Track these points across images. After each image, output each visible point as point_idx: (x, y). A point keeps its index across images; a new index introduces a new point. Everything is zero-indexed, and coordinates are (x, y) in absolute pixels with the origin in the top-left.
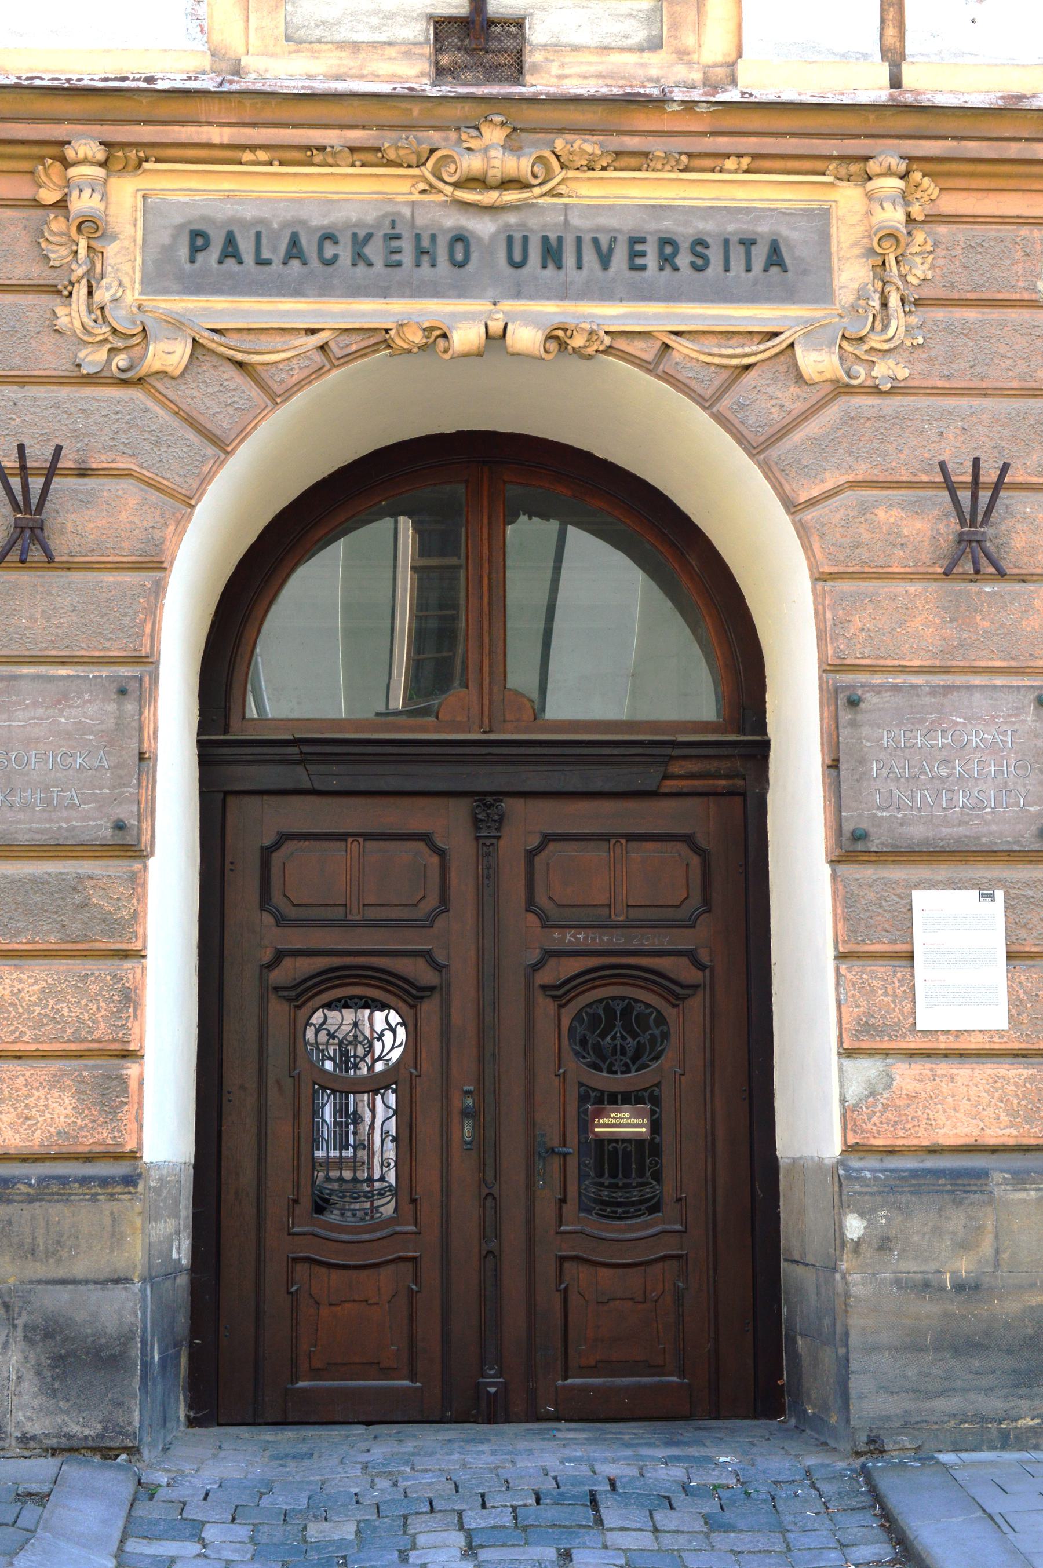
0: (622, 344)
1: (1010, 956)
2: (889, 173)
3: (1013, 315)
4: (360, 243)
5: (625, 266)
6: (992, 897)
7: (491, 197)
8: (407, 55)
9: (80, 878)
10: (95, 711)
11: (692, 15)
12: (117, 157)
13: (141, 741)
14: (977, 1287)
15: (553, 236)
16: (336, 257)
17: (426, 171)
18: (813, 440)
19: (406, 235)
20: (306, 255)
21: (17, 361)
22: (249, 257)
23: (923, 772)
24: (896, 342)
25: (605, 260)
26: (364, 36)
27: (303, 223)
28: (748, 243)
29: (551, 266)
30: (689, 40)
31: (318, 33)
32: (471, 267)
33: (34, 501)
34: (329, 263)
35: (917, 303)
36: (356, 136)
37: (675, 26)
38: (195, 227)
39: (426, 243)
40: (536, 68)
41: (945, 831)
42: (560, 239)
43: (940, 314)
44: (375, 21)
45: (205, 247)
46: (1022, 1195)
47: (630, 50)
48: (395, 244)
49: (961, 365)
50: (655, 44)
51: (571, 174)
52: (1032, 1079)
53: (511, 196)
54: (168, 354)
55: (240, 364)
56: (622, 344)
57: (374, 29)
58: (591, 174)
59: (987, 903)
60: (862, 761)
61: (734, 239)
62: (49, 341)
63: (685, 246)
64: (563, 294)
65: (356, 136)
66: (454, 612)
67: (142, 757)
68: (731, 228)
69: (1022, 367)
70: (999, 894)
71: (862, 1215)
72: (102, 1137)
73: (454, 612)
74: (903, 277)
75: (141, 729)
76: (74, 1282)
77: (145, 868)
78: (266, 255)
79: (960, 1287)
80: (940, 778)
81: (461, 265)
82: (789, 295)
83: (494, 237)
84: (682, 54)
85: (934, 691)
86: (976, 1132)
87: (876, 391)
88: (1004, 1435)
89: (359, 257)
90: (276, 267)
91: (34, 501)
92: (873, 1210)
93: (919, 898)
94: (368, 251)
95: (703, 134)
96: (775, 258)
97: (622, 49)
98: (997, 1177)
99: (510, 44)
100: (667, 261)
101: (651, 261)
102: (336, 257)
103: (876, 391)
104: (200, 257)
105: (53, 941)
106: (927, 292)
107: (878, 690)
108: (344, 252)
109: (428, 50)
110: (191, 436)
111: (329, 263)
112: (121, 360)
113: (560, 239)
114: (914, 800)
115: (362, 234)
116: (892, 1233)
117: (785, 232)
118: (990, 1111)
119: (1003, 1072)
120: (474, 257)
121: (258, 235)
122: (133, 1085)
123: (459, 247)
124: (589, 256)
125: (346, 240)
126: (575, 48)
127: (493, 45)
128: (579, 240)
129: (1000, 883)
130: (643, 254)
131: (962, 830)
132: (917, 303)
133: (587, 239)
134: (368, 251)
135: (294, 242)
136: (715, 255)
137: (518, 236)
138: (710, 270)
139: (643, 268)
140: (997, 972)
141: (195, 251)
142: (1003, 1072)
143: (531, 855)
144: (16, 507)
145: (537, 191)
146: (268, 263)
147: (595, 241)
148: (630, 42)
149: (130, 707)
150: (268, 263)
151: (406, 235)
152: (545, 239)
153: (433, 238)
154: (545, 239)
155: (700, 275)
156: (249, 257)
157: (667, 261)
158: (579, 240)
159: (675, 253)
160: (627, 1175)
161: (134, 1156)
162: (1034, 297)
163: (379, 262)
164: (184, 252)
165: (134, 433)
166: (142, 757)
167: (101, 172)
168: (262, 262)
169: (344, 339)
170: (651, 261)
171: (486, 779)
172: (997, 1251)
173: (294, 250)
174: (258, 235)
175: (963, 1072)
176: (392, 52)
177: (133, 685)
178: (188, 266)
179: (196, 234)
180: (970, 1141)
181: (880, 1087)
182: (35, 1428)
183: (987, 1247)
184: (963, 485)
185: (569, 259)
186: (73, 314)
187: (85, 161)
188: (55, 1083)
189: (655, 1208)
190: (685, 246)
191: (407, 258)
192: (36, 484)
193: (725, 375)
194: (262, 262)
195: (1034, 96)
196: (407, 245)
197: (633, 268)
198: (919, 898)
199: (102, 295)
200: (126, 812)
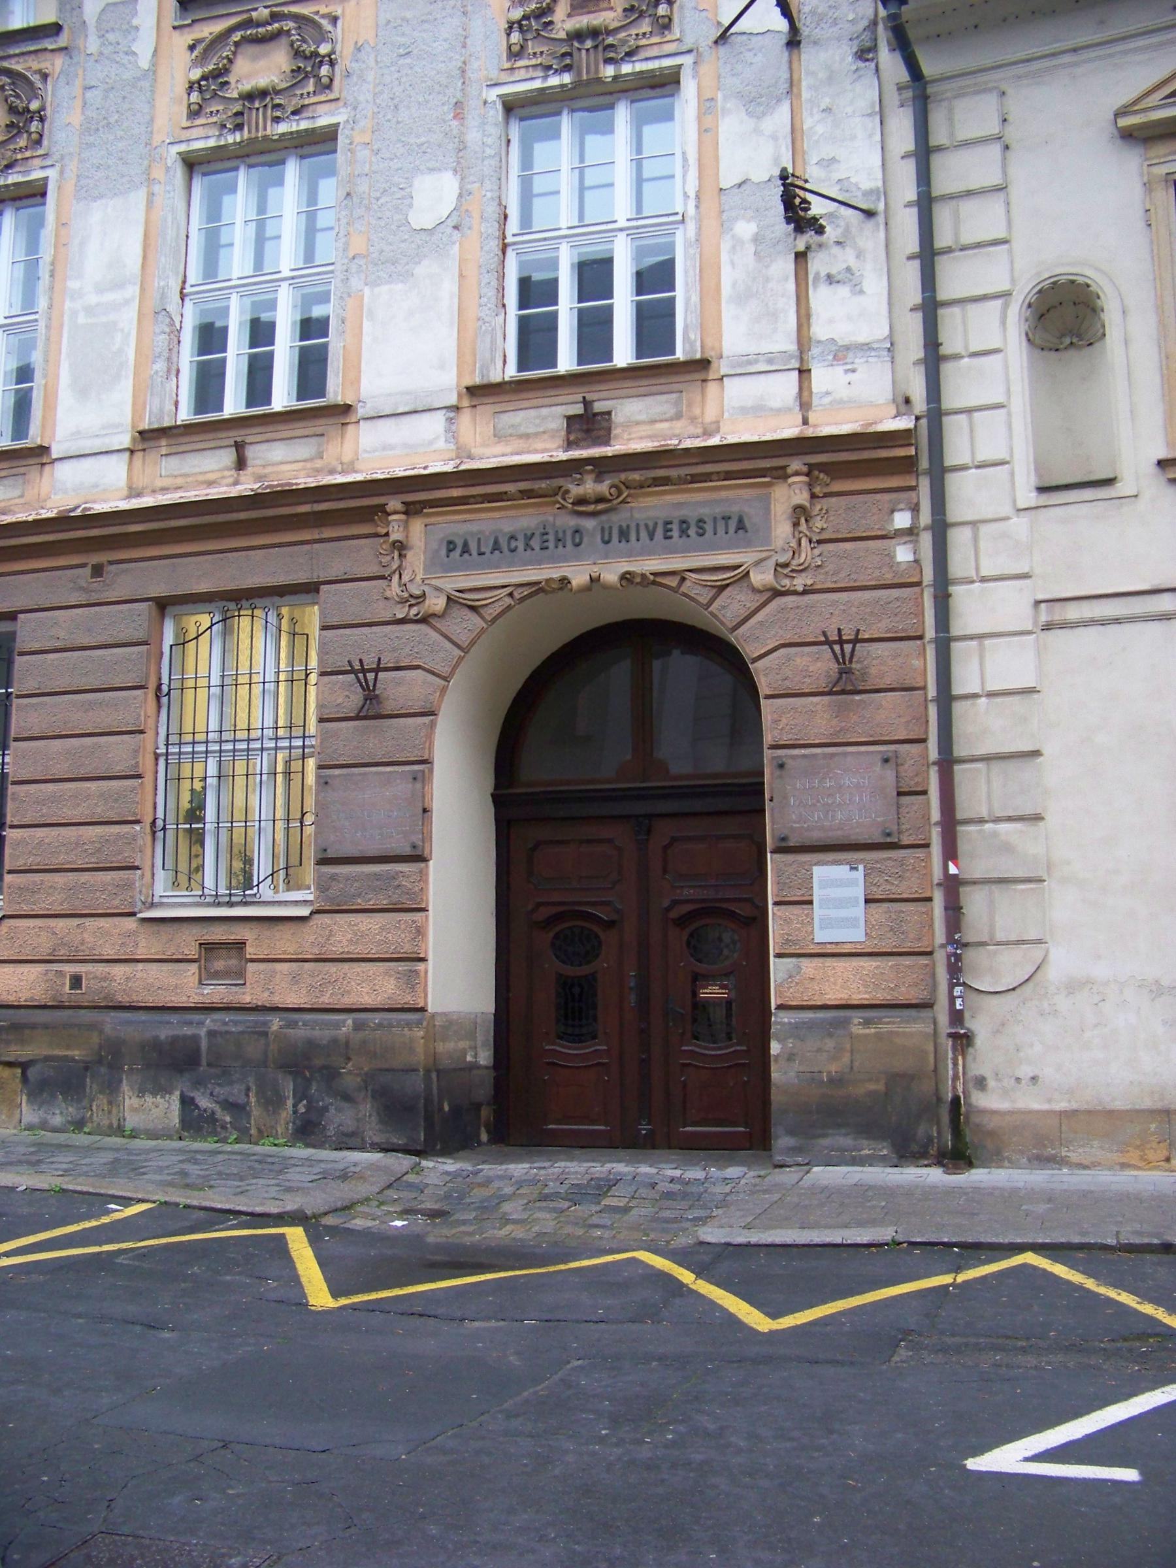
0: (659, 579)
1: (867, 901)
2: (797, 474)
3: (871, 544)
4: (529, 538)
5: (661, 536)
6: (856, 869)
7: (591, 508)
8: (553, 437)
9: (397, 873)
10: (403, 788)
11: (699, 398)
12: (411, 510)
13: (423, 802)
14: (840, 1080)
15: (624, 525)
16: (516, 547)
17: (559, 498)
18: (761, 623)
19: (551, 532)
20: (501, 548)
21: (369, 616)
22: (474, 552)
23: (818, 801)
24: (806, 565)
25: (651, 536)
26: (531, 430)
27: (501, 531)
28: (726, 518)
29: (624, 541)
30: (697, 411)
31: (510, 431)
32: (583, 546)
33: (371, 684)
34: (513, 551)
35: (819, 542)
36: (523, 486)
37: (690, 405)
38: (451, 538)
39: (561, 535)
40: (617, 437)
41: (830, 834)
42: (628, 526)
43: (831, 547)
44: (537, 421)
45: (454, 549)
46: (867, 1031)
47: (666, 420)
48: (545, 537)
49: (843, 574)
50: (678, 416)
51: (632, 491)
52: (877, 967)
53: (601, 507)
54: (437, 603)
55: (472, 608)
56: (659, 579)
57: (537, 426)
58: (644, 490)
59: (854, 873)
60: (785, 797)
61: (719, 517)
62: (382, 603)
63: (693, 523)
64: (630, 554)
65: (523, 486)
66: (201, 826)
67: (425, 811)
68: (717, 510)
69: (877, 573)
70: (861, 867)
71: (779, 1041)
72: (407, 999)
73: (201, 826)
74: (809, 528)
75: (423, 797)
76: (393, 1070)
77: (427, 866)
78: (483, 550)
79: (831, 1081)
80: (828, 804)
81: (578, 545)
82: (749, 544)
83: (594, 528)
84: (693, 420)
85: (825, 756)
86: (846, 997)
87: (795, 593)
88: (854, 1158)
89: (528, 546)
90: (488, 554)
91: (371, 684)
92: (786, 1039)
93: (817, 871)
94: (532, 543)
95: (697, 464)
96: (741, 526)
97: (661, 421)
98: (856, 1021)
99: (605, 424)
100: (684, 532)
101: (675, 533)
102: (516, 547)
103: (795, 593)
104: (452, 554)
105: (384, 903)
106: (825, 536)
107: (794, 757)
108: (520, 545)
109: (563, 433)
110: (448, 645)
111: (513, 551)
112: (414, 611)
113: (628, 526)
114: (813, 817)
115: (529, 533)
116: (795, 1051)
117: (746, 510)
118: (854, 985)
119: (862, 964)
120: (585, 540)
121: (479, 539)
122: (422, 974)
123: (577, 535)
124: (644, 534)
125: (521, 538)
126: (638, 423)
127: (597, 426)
128: (638, 525)
129: (862, 861)
130: (671, 530)
131: (840, 833)
132: (819, 542)
133: (642, 524)
134: (532, 543)
135: (496, 542)
136: (709, 527)
137: (607, 526)
138: (706, 535)
139: (671, 537)
140: (860, 910)
141: (450, 551)
142: (862, 964)
143: (666, 848)
144: (364, 690)
145: (615, 502)
146: (484, 554)
147: (647, 526)
148: (667, 416)
149: (418, 785)
150: (484, 554)
151: (551, 532)
152: (620, 527)
153: (564, 532)
154: (620, 527)
155: (701, 538)
156: (474, 552)
157: (684, 532)
158: (638, 525)
159: (688, 528)
160: (580, 1019)
161: (423, 1010)
162: (884, 533)
163: (537, 548)
164: (444, 552)
165: (421, 646)
166: (425, 811)
167: (403, 517)
168: (481, 554)
169: (520, 590)
170: (675, 533)
171: (640, 808)
172: (852, 1062)
173: (496, 547)
174: (479, 539)
175: (840, 964)
176: (546, 436)
177: (419, 776)
178: (446, 559)
179: (450, 542)
180: (844, 1002)
181: (794, 974)
182: (376, 1139)
183: (846, 1059)
184: (835, 642)
185: (633, 537)
186: (395, 589)
187: (395, 513)
188: (386, 973)
189: (594, 1038)
190: (693, 523)
191: (551, 545)
192: (370, 676)
193: (715, 590)
194: (481, 554)
195: (875, 423)
196: (551, 537)
197: (666, 538)
198: (817, 871)
199: (405, 578)
200: (416, 839)
